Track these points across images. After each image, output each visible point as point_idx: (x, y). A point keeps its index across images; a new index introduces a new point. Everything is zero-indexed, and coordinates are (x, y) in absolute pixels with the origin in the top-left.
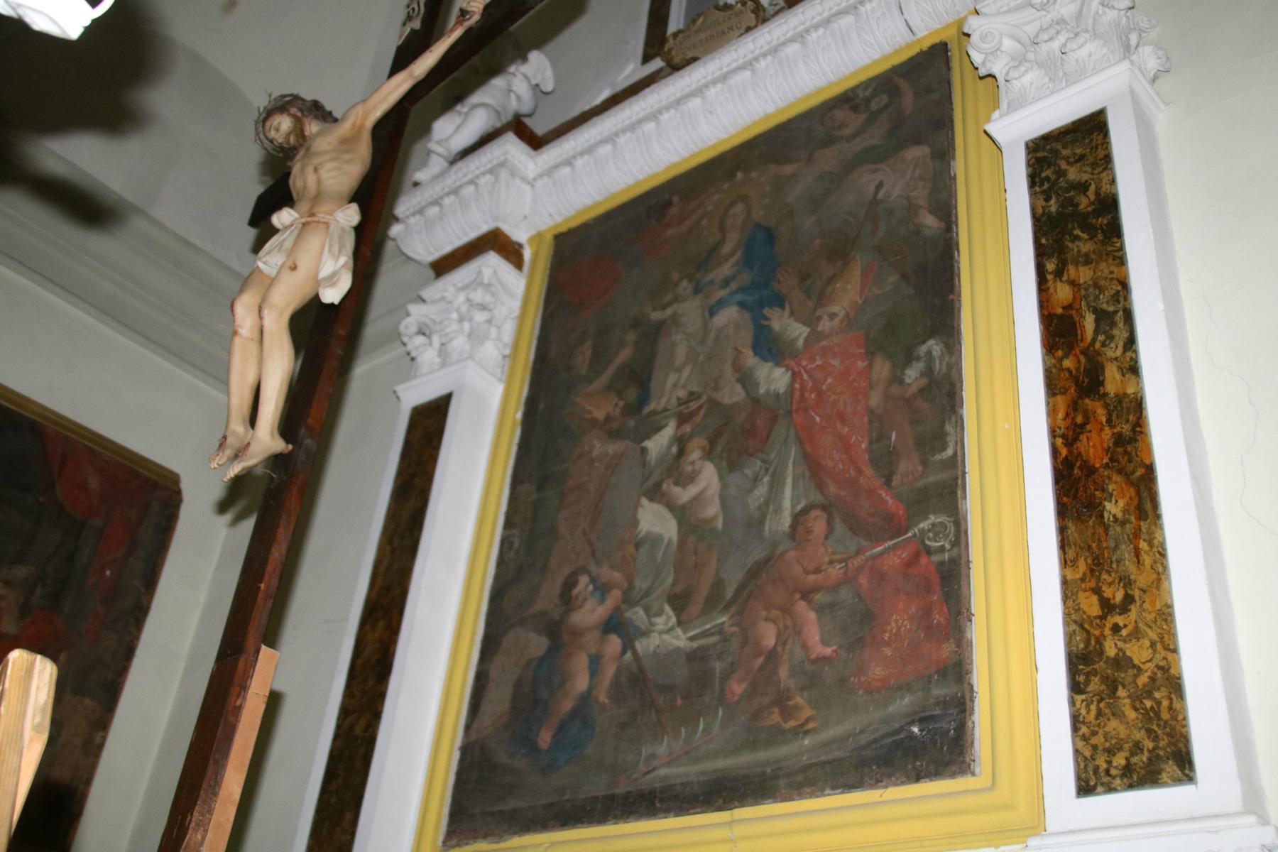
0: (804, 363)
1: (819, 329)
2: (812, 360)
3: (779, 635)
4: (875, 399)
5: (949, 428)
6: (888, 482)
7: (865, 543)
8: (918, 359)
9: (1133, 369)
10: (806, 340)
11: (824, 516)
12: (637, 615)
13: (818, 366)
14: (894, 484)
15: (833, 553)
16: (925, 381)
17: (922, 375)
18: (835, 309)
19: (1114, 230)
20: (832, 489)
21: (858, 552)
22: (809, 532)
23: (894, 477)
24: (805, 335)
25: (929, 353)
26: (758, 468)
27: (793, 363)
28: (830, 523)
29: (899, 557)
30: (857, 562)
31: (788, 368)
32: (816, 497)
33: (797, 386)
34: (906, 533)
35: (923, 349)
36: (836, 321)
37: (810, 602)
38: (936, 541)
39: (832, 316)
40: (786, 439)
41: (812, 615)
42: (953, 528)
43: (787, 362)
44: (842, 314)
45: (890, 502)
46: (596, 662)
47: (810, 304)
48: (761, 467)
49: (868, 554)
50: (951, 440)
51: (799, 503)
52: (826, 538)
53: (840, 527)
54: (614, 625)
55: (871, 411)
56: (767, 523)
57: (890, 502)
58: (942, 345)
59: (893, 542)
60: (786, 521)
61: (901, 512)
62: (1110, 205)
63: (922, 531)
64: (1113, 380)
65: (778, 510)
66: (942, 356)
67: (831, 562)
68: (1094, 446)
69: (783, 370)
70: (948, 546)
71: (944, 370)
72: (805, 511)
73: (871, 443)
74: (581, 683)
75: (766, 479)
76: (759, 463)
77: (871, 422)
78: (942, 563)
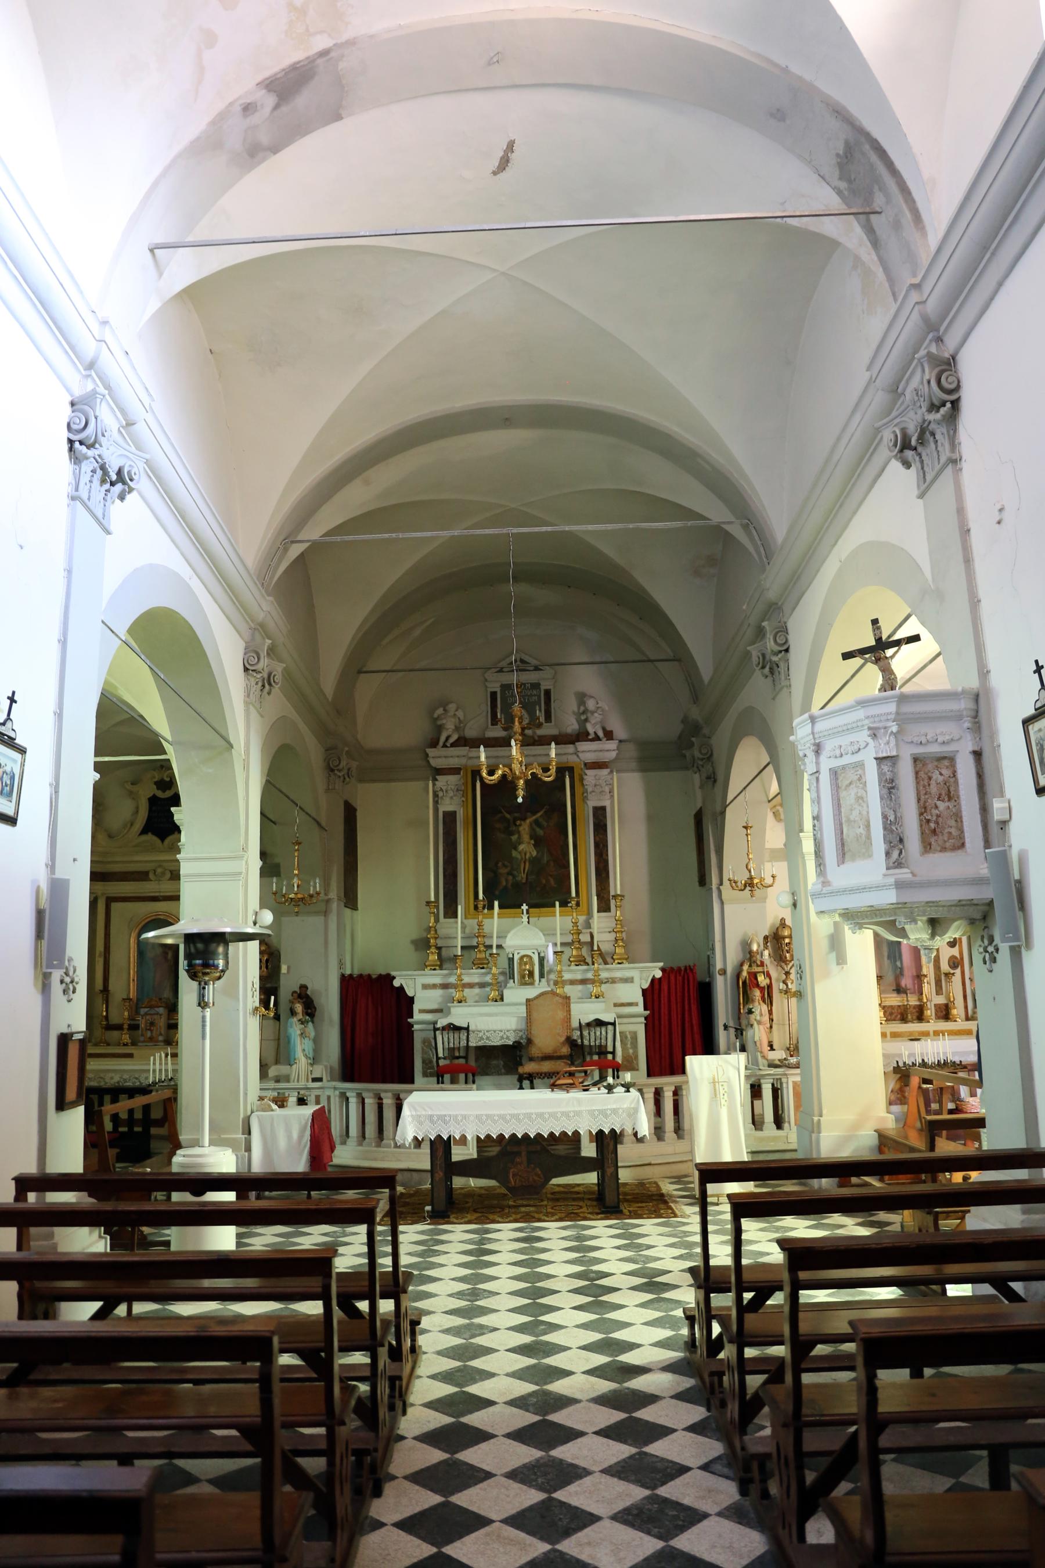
9: (607, 855)
12: (515, 873)
19: (606, 831)
46: (507, 880)
54: (510, 873)
60: (545, 862)
62: (605, 825)
64: (604, 856)
68: (601, 865)
74: (504, 883)
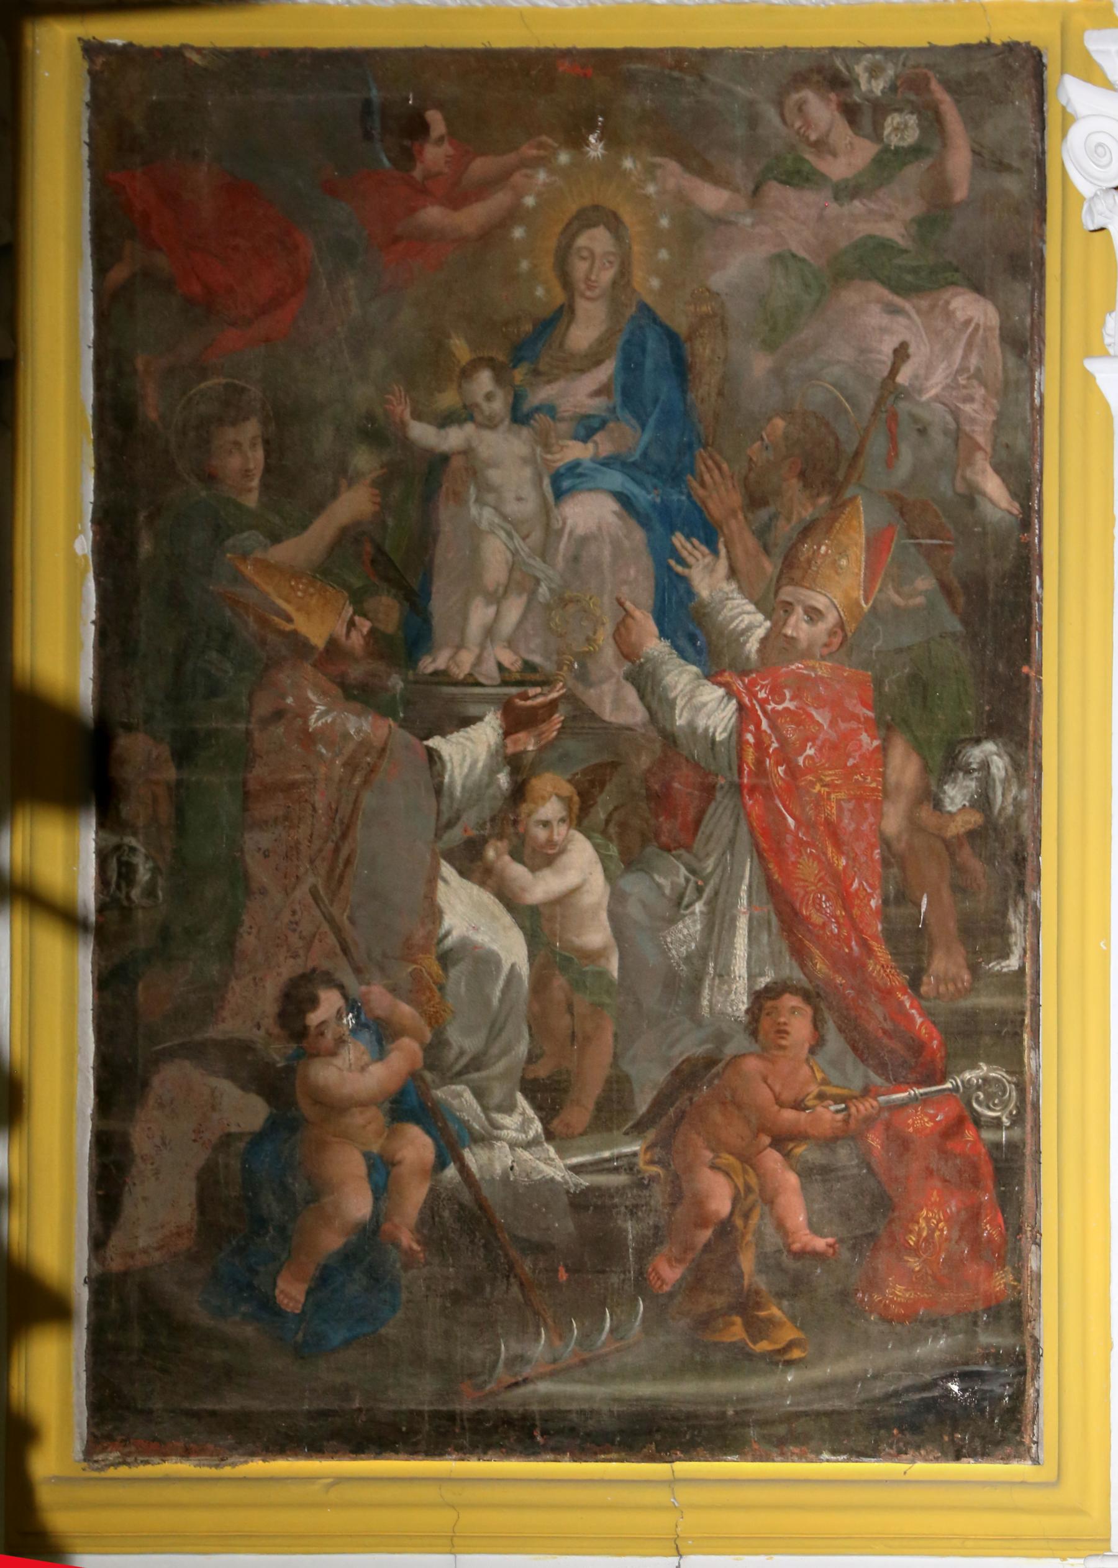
0: (762, 695)
1: (789, 631)
2: (776, 692)
3: (736, 1200)
4: (893, 821)
5: (1014, 921)
6: (915, 984)
7: (878, 1080)
8: (968, 772)
10: (764, 641)
11: (809, 1011)
13: (786, 709)
14: (924, 989)
15: (825, 1082)
16: (975, 819)
17: (973, 805)
18: (820, 601)
20: (821, 966)
21: (867, 1092)
22: (782, 1032)
23: (925, 979)
24: (760, 632)
25: (985, 766)
26: (682, 881)
27: (739, 685)
28: (817, 1023)
29: (932, 1118)
30: (865, 1107)
31: (731, 693)
32: (791, 971)
33: (750, 738)
34: (943, 1081)
35: (975, 755)
36: (823, 627)
37: (787, 1155)
38: (989, 1108)
39: (814, 614)
40: (732, 842)
41: (792, 1179)
42: (1014, 1094)
43: (727, 677)
44: (831, 619)
45: (919, 1020)
47: (770, 567)
48: (687, 880)
49: (882, 1099)
50: (1017, 941)
51: (762, 974)
52: (812, 1051)
53: (834, 1041)
55: (886, 843)
56: (706, 992)
57: (919, 1020)
58: (1007, 759)
59: (922, 1091)
60: (741, 1004)
61: (935, 1043)
63: (967, 1084)
65: (724, 975)
66: (1006, 781)
67: (821, 1097)
69: (721, 692)
70: (1006, 1122)
71: (1010, 809)
72: (773, 992)
73: (886, 902)
75: (698, 907)
76: (683, 871)
77: (886, 863)
78: (997, 1145)
